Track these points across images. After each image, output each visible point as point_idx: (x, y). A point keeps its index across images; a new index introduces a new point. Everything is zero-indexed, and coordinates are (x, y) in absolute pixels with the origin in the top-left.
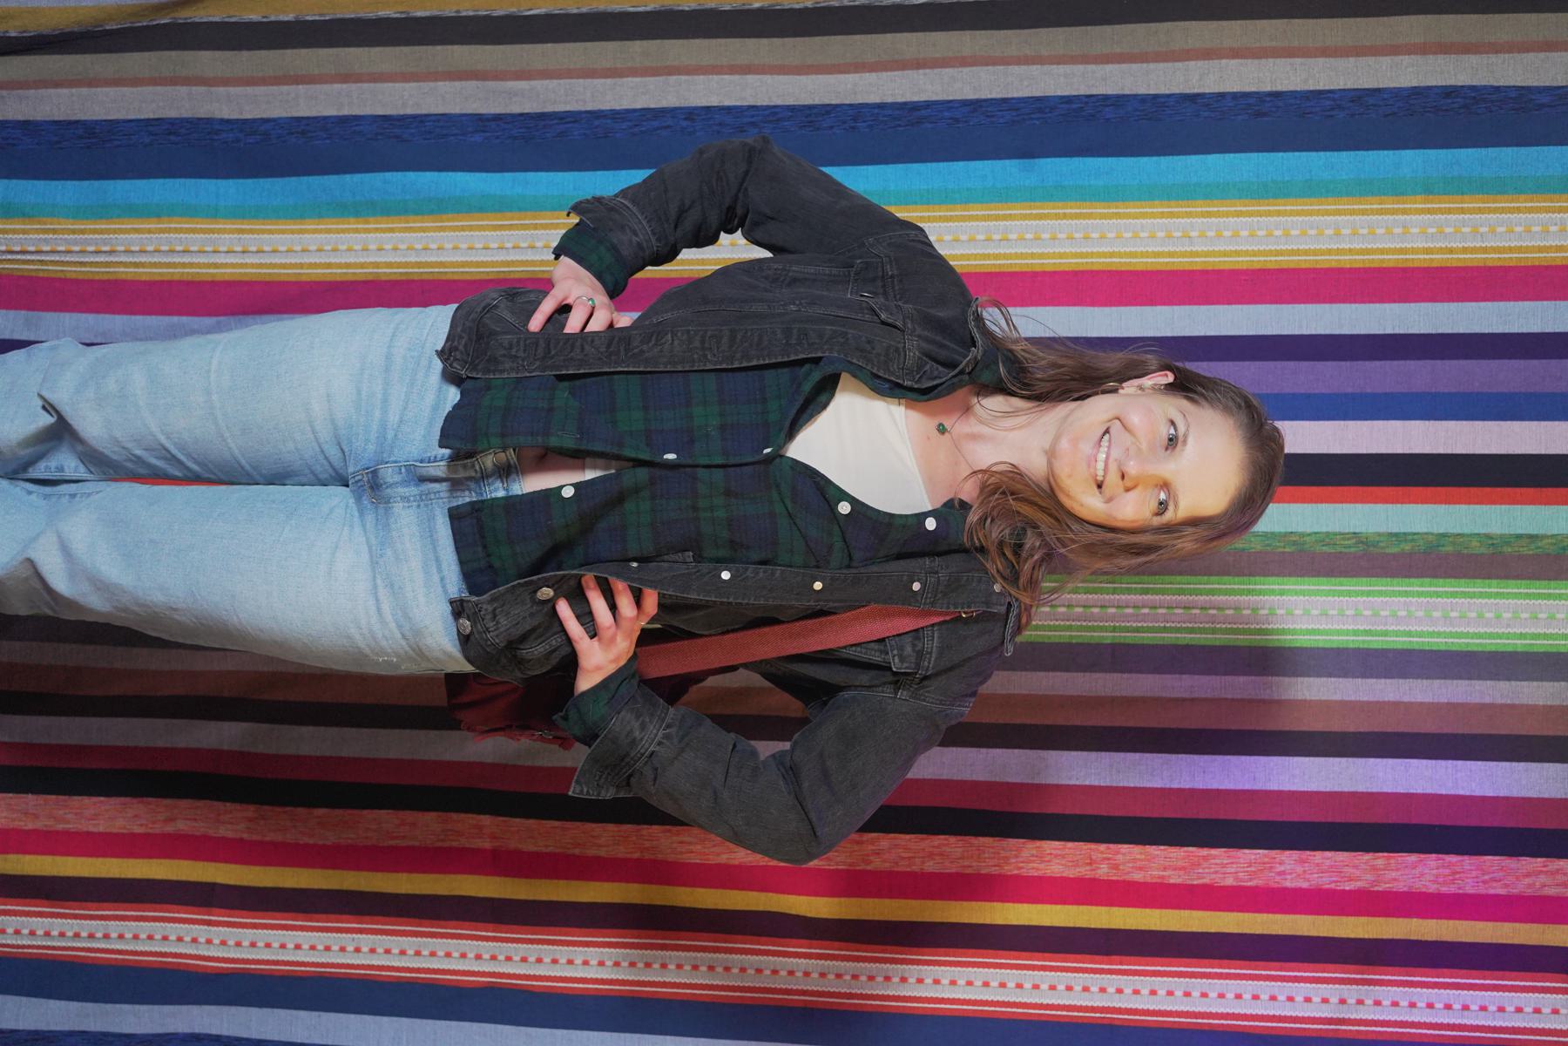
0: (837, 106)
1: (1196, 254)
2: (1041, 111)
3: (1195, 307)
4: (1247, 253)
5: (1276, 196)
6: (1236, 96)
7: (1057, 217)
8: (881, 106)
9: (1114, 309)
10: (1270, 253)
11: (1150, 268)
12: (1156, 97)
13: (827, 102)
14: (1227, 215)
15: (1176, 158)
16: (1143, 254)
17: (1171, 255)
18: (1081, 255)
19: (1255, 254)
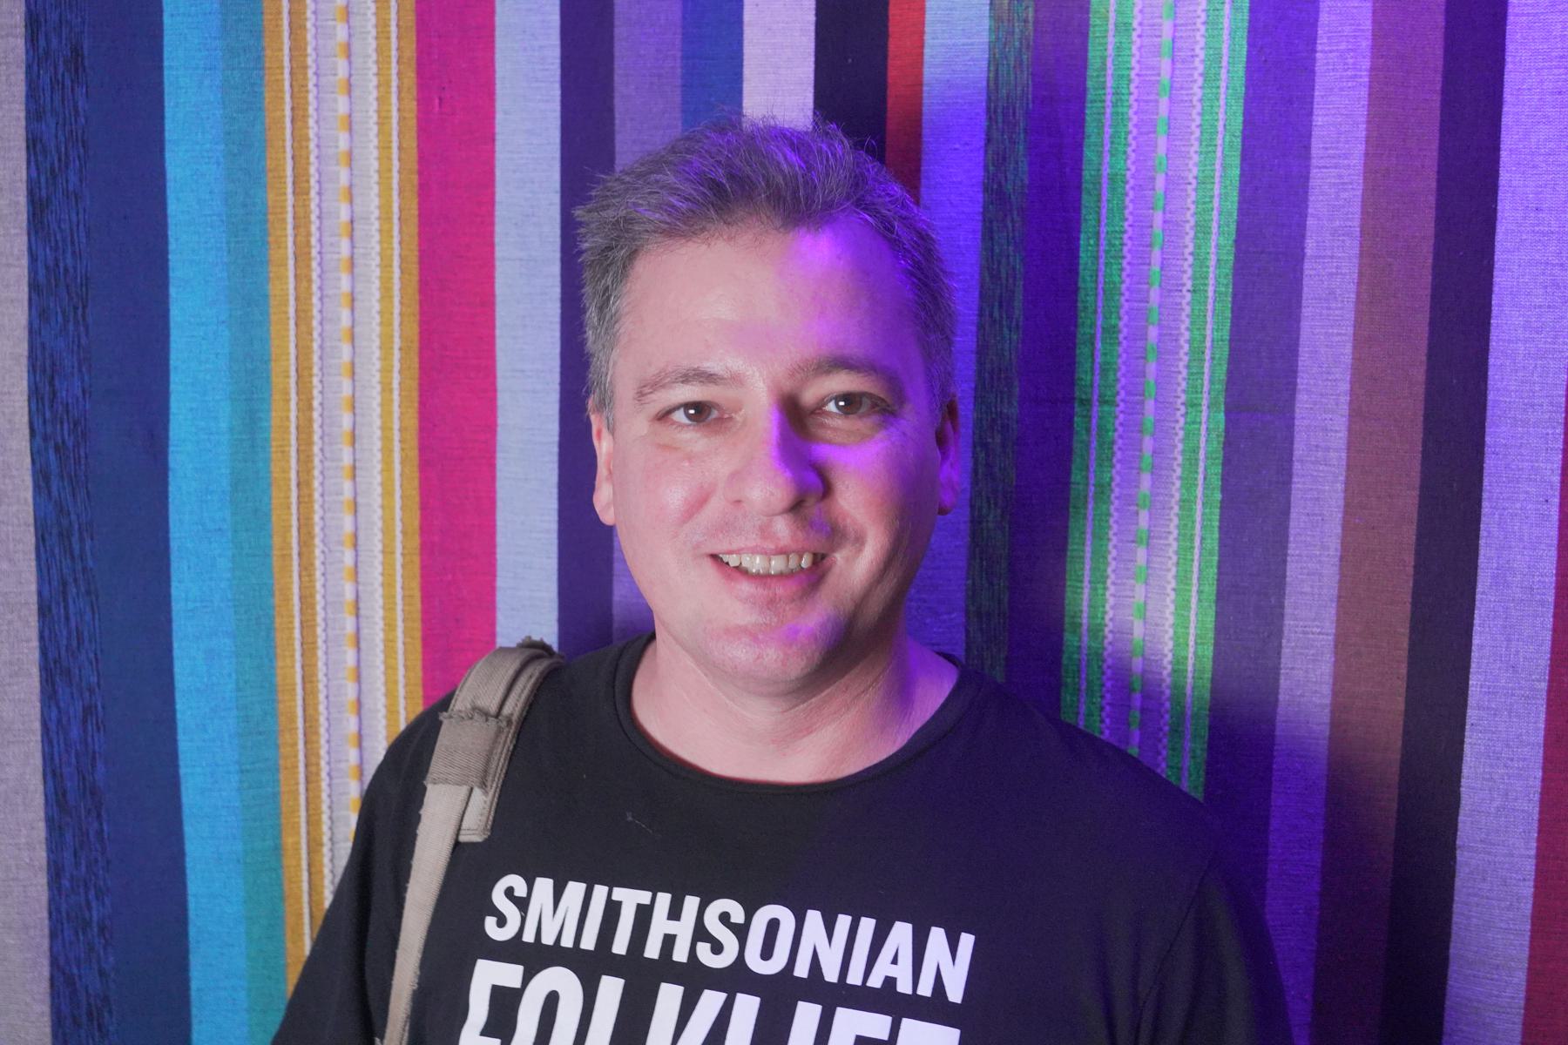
0: (54, 962)
1: (385, 208)
2: (65, 535)
3: (500, 212)
4: (382, 100)
5: (257, 33)
6: (35, 113)
7: (305, 501)
8: (55, 872)
9: (501, 383)
10: (381, 50)
11: (415, 308)
12: (34, 286)
13: (44, 986)
14: (300, 140)
15: (172, 246)
16: (386, 323)
17: (385, 265)
18: (387, 451)
19: (383, 85)
